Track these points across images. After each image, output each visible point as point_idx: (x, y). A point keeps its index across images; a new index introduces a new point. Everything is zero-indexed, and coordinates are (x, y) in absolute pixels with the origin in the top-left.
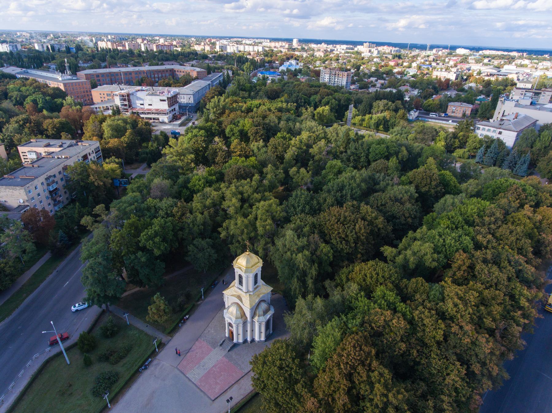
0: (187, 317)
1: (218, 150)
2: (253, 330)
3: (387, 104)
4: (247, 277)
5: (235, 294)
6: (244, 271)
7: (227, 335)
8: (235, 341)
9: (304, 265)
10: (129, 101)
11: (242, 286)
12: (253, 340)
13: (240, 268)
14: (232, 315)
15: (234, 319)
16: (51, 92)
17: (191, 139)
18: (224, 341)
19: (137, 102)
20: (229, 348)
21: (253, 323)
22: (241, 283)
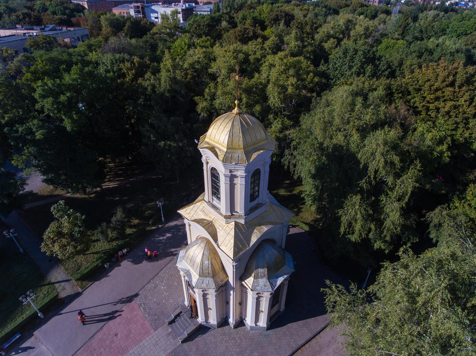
0: (125, 251)
1: (223, 32)
2: (242, 303)
3: (438, 15)
4: (232, 178)
5: (203, 217)
6: (221, 157)
7: (186, 303)
8: (201, 319)
9: (386, 162)
10: (144, 13)
11: (219, 198)
12: (240, 323)
13: (213, 149)
14: (193, 266)
15: (195, 278)
16: (72, 6)
17: (192, 25)
18: (178, 315)
19: (152, 15)
20: (186, 335)
21: (243, 290)
22: (216, 192)
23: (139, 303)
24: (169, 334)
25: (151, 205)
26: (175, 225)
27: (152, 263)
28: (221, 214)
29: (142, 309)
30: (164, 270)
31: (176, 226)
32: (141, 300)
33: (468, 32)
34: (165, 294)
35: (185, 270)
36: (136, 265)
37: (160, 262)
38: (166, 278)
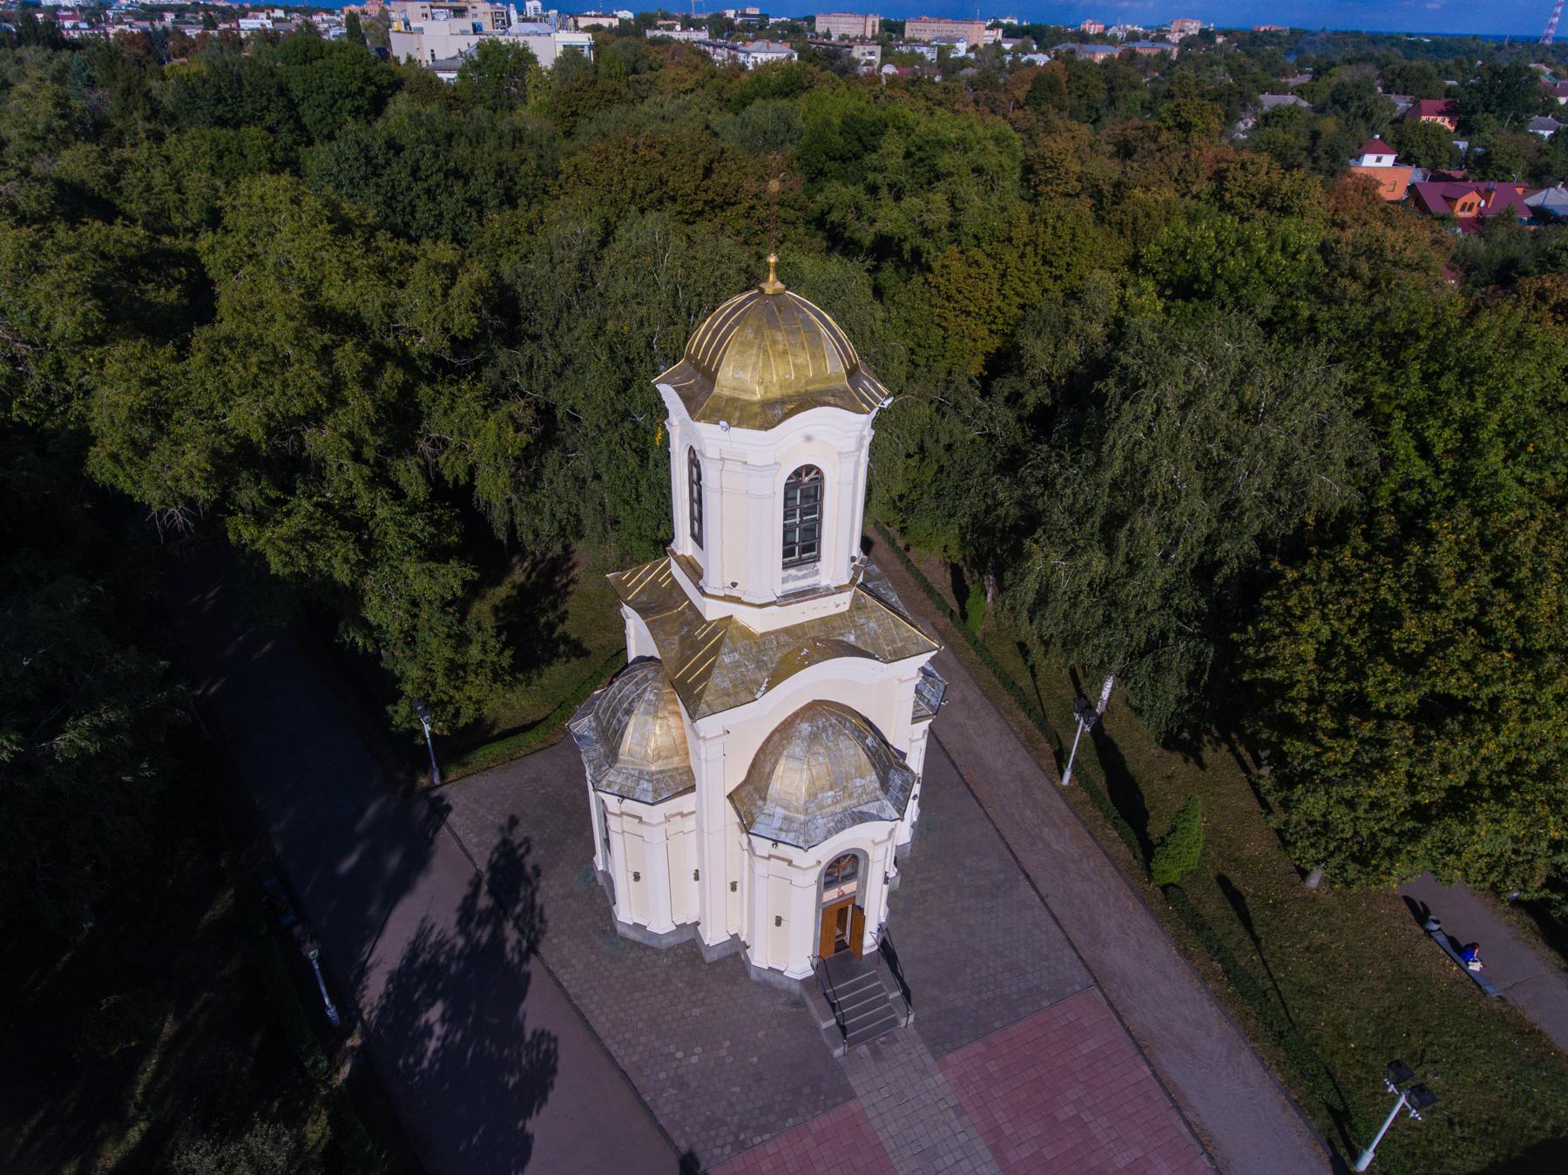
18: (833, 1005)
23: (728, 1150)
24: (876, 1053)
25: (157, 1075)
26: (390, 980)
27: (551, 1096)
28: (840, 589)
29: (757, 1140)
30: (613, 1049)
31: (397, 978)
32: (719, 1142)
33: (353, 88)
34: (724, 1053)
35: (841, 821)
36: (532, 1164)
37: (564, 1061)
38: (657, 1044)
